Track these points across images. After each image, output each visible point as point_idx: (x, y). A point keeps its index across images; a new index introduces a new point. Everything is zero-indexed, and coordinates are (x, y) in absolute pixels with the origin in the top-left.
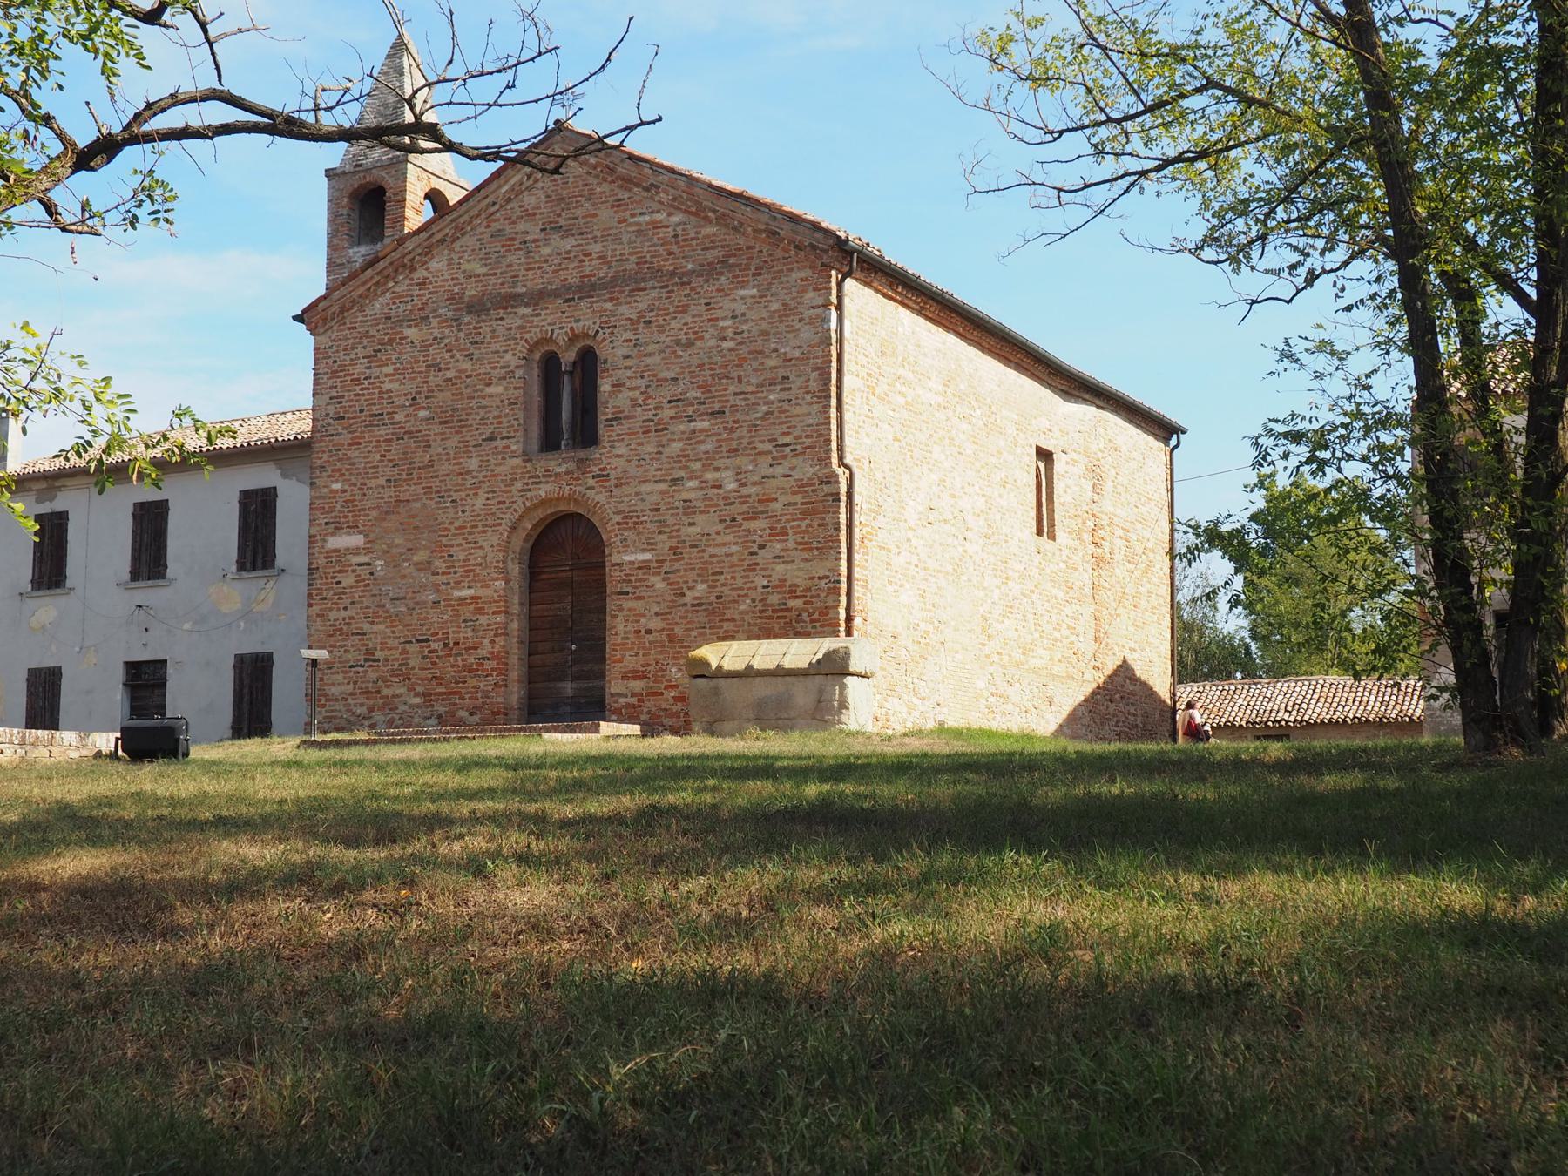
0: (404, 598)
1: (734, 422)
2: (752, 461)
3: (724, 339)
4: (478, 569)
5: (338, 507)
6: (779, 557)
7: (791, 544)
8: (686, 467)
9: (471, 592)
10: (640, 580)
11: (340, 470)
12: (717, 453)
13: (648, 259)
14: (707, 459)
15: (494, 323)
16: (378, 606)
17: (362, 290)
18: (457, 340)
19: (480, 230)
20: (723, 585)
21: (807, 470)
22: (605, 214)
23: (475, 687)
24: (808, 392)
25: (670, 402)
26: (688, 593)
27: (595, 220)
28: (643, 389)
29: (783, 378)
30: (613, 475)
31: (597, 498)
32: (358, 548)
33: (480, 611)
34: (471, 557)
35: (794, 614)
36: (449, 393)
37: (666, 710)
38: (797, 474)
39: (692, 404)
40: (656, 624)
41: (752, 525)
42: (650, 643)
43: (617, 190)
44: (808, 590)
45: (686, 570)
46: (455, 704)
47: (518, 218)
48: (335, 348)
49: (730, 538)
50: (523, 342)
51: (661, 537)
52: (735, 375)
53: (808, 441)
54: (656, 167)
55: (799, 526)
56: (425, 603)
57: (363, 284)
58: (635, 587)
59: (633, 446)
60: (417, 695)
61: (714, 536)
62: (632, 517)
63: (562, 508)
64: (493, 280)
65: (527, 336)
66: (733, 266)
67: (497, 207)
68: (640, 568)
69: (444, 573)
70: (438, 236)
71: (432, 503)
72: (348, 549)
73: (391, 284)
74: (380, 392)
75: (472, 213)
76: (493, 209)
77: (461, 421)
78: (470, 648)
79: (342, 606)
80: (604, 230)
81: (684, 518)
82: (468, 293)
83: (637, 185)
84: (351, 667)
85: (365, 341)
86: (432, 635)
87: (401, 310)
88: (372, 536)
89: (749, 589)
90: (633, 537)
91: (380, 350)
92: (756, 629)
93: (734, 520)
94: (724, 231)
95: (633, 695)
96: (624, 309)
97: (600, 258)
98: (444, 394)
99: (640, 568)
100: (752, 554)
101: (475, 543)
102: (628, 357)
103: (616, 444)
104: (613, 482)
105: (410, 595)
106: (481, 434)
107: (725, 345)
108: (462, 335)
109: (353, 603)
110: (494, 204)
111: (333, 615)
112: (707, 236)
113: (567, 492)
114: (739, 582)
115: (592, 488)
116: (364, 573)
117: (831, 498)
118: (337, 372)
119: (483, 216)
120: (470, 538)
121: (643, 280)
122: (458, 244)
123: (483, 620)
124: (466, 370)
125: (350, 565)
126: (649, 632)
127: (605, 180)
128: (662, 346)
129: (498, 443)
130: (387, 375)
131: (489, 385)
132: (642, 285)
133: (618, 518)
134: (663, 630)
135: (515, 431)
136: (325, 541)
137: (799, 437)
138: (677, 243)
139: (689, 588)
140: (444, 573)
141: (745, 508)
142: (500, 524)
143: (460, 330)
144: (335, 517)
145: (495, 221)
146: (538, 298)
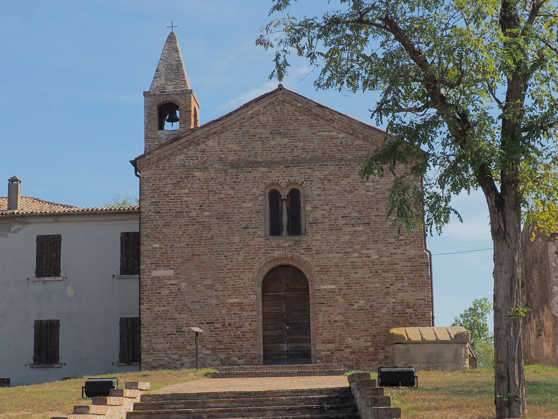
0: (199, 302)
1: (376, 228)
2: (385, 246)
3: (369, 191)
4: (241, 289)
5: (158, 256)
6: (400, 290)
7: (406, 284)
8: (352, 247)
9: (238, 300)
10: (330, 298)
11: (158, 238)
12: (368, 242)
13: (328, 151)
14: (362, 244)
15: (246, 174)
16: (184, 305)
17: (170, 152)
18: (225, 180)
19: (235, 130)
20: (373, 301)
21: (412, 252)
22: (305, 130)
23: (241, 346)
25: (342, 217)
26: (355, 304)
27: (299, 131)
28: (328, 210)
30: (314, 248)
31: (306, 259)
32: (171, 277)
33: (243, 309)
34: (237, 283)
35: (409, 315)
36: (222, 205)
37: (346, 357)
38: (408, 253)
39: (354, 219)
41: (386, 275)
43: (310, 119)
44: (415, 305)
45: (354, 294)
47: (257, 126)
48: (153, 178)
49: (376, 280)
50: (263, 184)
51: (340, 278)
52: (375, 207)
53: (412, 239)
54: (332, 111)
55: (410, 276)
56: (211, 305)
57: (171, 149)
58: (328, 301)
59: (324, 236)
62: (325, 268)
63: (284, 262)
64: (244, 153)
65: (265, 181)
67: (246, 120)
68: (329, 292)
69: (221, 291)
70: (214, 130)
71: (214, 256)
72: (164, 277)
73: (186, 150)
74: (181, 202)
75: (232, 122)
76: (243, 121)
77: (229, 218)
78: (238, 327)
79: (162, 305)
80: (305, 136)
82: (230, 158)
83: (322, 118)
84: (168, 335)
86: (215, 320)
87: (191, 163)
88: (178, 271)
89: (386, 303)
90: (326, 278)
91: (181, 182)
92: (390, 321)
93: (377, 272)
94: (366, 143)
95: (328, 350)
96: (316, 173)
97: (302, 149)
98: (219, 205)
99: (329, 292)
100: (387, 288)
101: (239, 277)
102: (320, 195)
103: (315, 234)
104: (314, 252)
105: (202, 300)
106: (240, 225)
107: (369, 193)
108: (228, 178)
109: (168, 303)
110: (244, 118)
111: (156, 309)
112: (358, 145)
113: (289, 256)
114: (381, 300)
116: (175, 289)
117: (424, 265)
118: (155, 190)
119: (238, 123)
120: (236, 275)
122: (223, 136)
123: (245, 314)
124: (231, 195)
125: (166, 285)
126: (336, 321)
127: (304, 114)
128: (337, 192)
129: (250, 230)
130: (185, 194)
131: (245, 202)
132: (326, 163)
133: (317, 269)
134: (343, 321)
135: (259, 225)
138: (342, 146)
139: (356, 302)
140: (221, 291)
141: (383, 267)
142: (253, 269)
143: (227, 176)
144: (157, 261)
146: (270, 164)
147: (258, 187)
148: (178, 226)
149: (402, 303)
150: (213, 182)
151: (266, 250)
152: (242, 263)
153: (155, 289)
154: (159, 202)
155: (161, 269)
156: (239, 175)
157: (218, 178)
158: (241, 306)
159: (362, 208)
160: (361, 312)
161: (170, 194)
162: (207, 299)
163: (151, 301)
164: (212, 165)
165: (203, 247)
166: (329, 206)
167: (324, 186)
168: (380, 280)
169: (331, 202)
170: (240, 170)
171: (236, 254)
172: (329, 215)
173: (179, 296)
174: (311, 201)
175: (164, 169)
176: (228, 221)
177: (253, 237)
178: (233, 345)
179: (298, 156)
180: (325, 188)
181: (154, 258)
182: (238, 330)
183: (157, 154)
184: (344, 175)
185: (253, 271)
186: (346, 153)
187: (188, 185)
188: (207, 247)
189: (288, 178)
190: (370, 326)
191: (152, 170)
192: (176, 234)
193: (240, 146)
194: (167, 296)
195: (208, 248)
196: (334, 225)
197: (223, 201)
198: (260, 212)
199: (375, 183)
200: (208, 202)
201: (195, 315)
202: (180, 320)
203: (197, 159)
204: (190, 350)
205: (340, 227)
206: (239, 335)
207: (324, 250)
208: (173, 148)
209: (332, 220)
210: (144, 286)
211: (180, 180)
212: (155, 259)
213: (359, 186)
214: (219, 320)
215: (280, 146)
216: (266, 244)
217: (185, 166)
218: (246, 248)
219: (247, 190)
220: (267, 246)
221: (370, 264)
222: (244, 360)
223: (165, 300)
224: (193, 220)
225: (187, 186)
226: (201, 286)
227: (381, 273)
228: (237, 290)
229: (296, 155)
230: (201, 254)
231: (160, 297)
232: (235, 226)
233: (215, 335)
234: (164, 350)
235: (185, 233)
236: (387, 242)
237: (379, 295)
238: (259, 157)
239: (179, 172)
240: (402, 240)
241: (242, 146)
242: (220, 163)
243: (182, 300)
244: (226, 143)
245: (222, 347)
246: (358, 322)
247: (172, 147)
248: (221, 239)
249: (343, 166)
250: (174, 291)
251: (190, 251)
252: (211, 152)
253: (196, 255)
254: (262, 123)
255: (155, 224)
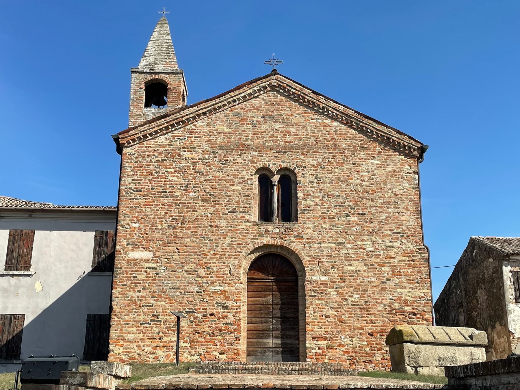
2: (381, 239)
6: (398, 286)
7: (403, 280)
8: (345, 238)
10: (322, 290)
12: (363, 233)
16: (161, 292)
19: (226, 112)
20: (368, 296)
24: (409, 210)
25: (336, 206)
29: (395, 202)
30: (305, 237)
33: (228, 299)
40: (331, 312)
42: (329, 322)
45: (347, 288)
46: (210, 348)
47: (248, 110)
49: (372, 273)
50: (253, 167)
53: (409, 233)
60: (185, 342)
61: (362, 272)
62: (316, 259)
63: (273, 250)
65: (255, 165)
66: (366, 149)
71: (197, 240)
72: (142, 260)
79: (136, 290)
81: (345, 262)
84: (141, 324)
85: (156, 155)
88: (158, 253)
89: (383, 299)
91: (166, 160)
93: (372, 265)
95: (319, 349)
97: (295, 135)
100: (383, 283)
102: (312, 182)
103: (307, 222)
105: (182, 287)
107: (364, 183)
109: (144, 288)
111: (131, 293)
114: (377, 296)
115: (294, 242)
116: (152, 273)
117: (423, 260)
118: (138, 167)
121: (319, 148)
122: (213, 117)
124: (219, 176)
125: (143, 268)
126: (327, 317)
131: (233, 185)
132: (319, 151)
136: (126, 254)
137: (404, 230)
139: (350, 296)
141: (378, 260)
142: (239, 255)
145: (234, 109)
146: (260, 149)
147: (248, 170)
148: (161, 206)
149: (400, 300)
150: (201, 163)
151: (254, 236)
152: (228, 248)
153: (130, 272)
154: (141, 180)
155: (139, 251)
156: (228, 157)
157: (206, 159)
158: (225, 295)
159: (357, 198)
160: (355, 308)
161: (154, 172)
162: (187, 286)
163: (126, 285)
164: (200, 146)
165: (186, 229)
166: (321, 194)
167: (317, 173)
168: (376, 274)
169: (324, 190)
170: (229, 152)
171: (222, 239)
172: (322, 203)
173: (157, 281)
174: (303, 188)
175: (148, 147)
176: (214, 204)
177: (241, 222)
178: (214, 338)
179: (290, 142)
180: (317, 175)
181: (132, 239)
182: (221, 321)
183: (142, 130)
184: (338, 163)
185: (239, 257)
186: (340, 142)
187: (174, 164)
188: (191, 230)
189: (279, 163)
190: (366, 324)
191: (135, 147)
192: (158, 214)
193: (230, 129)
194: (144, 280)
195: (192, 230)
196: (327, 214)
197: (210, 183)
198: (249, 196)
199: (370, 173)
200: (194, 183)
201: (173, 303)
202: (156, 307)
203: (185, 139)
204: (166, 342)
205: (333, 216)
206: (221, 327)
207: (316, 239)
208: (160, 125)
209: (325, 208)
210: (118, 268)
211: (166, 158)
212: (133, 240)
213: (353, 175)
214: (200, 309)
215: (272, 131)
216: (254, 229)
217: (172, 145)
218: (232, 232)
219: (236, 173)
220: (255, 232)
221: (366, 257)
222: (226, 355)
223: (141, 285)
224: (177, 200)
225: (172, 165)
226: (183, 271)
227: (376, 266)
228: (221, 277)
229: (288, 140)
230: (184, 236)
231: (135, 281)
232: (222, 209)
233: (194, 326)
234: (135, 341)
235: (167, 213)
236: (383, 234)
237: (374, 291)
238: (249, 140)
239: (164, 150)
240: (399, 233)
241: (232, 128)
242: (209, 144)
243: (160, 286)
244: (215, 125)
245: (202, 339)
246: (352, 319)
247: (159, 124)
248: (206, 223)
249: (337, 155)
250: (151, 275)
251: (172, 233)
252: (200, 132)
253: (179, 238)
254: (254, 107)
255: (135, 202)
